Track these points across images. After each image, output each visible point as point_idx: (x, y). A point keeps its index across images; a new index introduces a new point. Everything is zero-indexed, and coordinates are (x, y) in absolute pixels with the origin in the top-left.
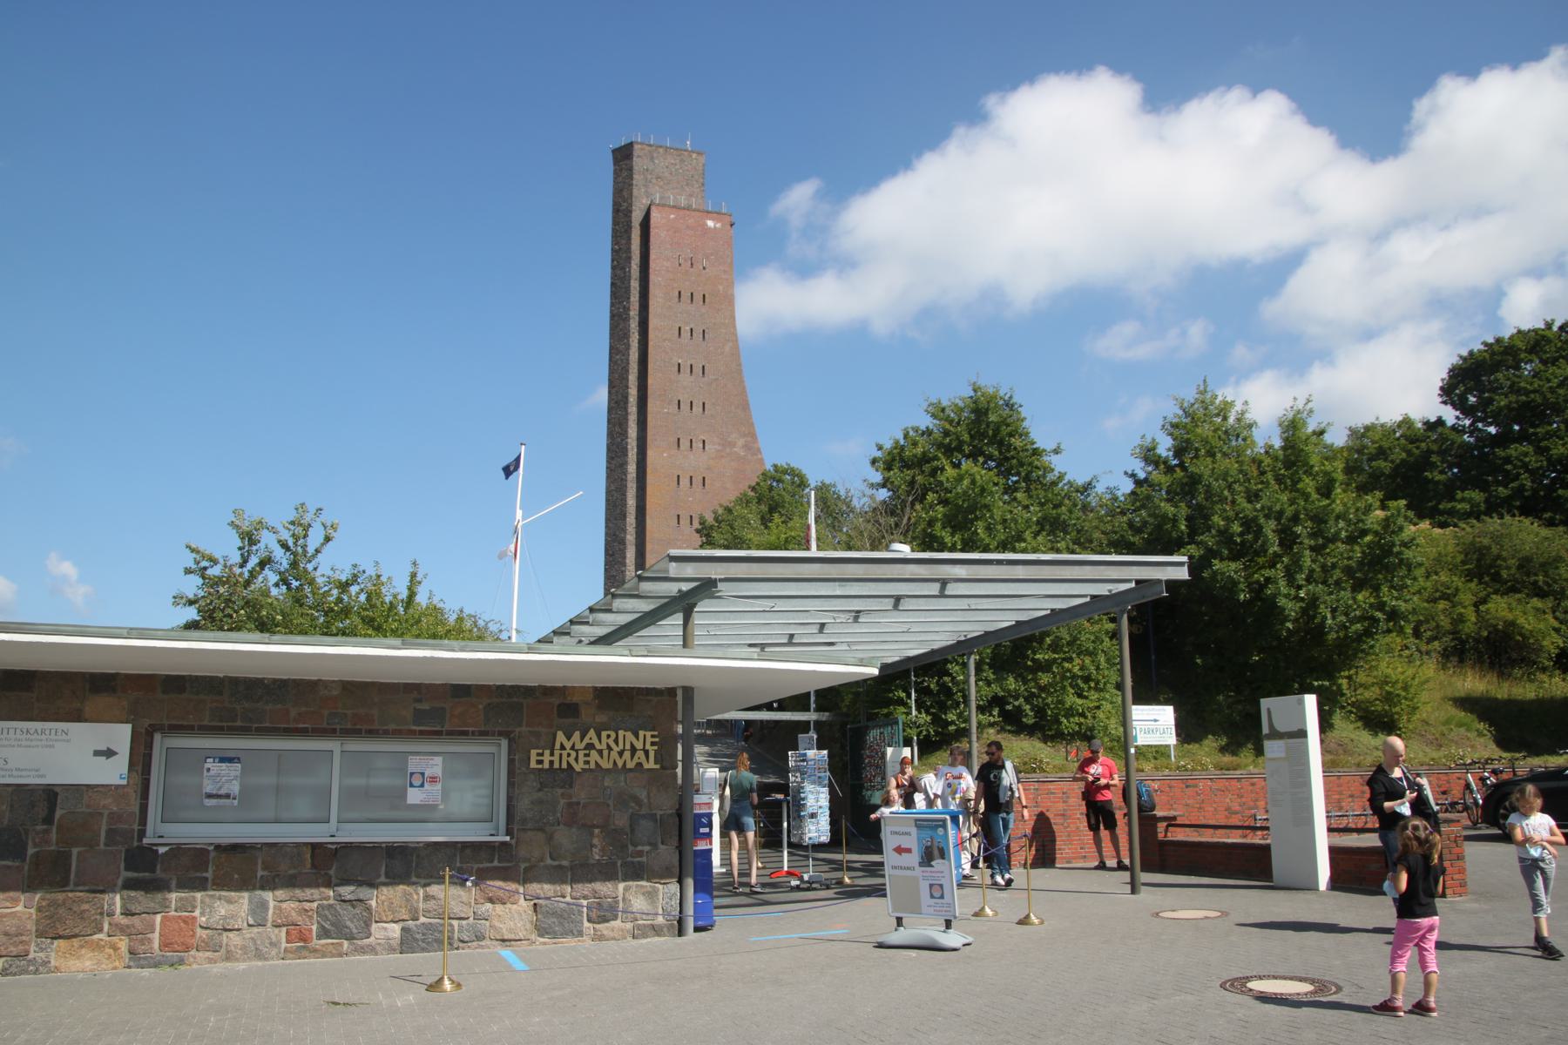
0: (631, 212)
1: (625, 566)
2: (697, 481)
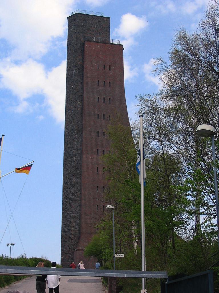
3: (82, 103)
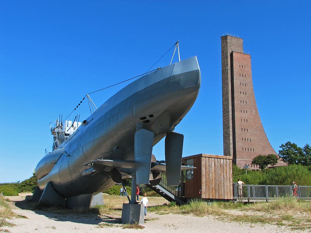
0: (227, 53)
2: (246, 120)
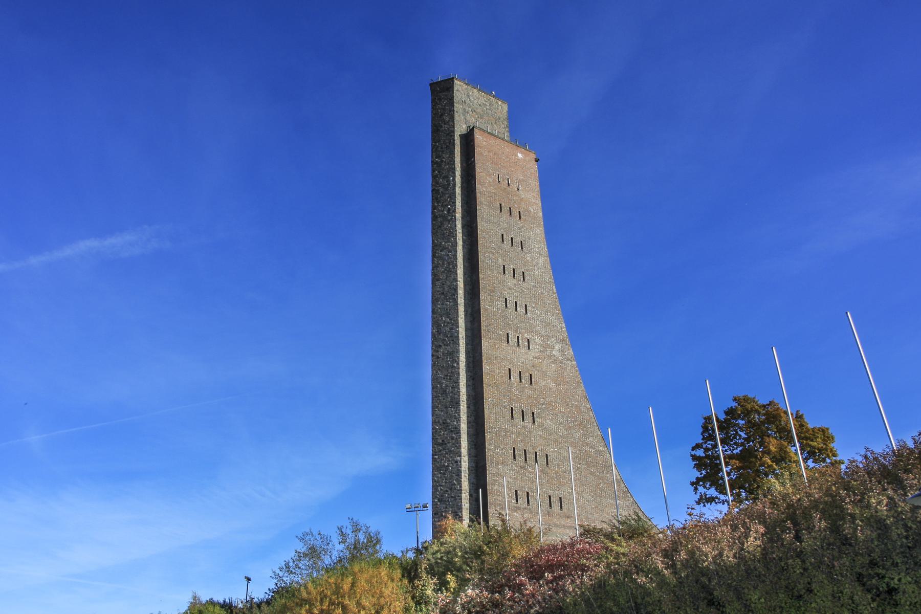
1: (460, 456)
2: (526, 376)
3: (469, 239)
